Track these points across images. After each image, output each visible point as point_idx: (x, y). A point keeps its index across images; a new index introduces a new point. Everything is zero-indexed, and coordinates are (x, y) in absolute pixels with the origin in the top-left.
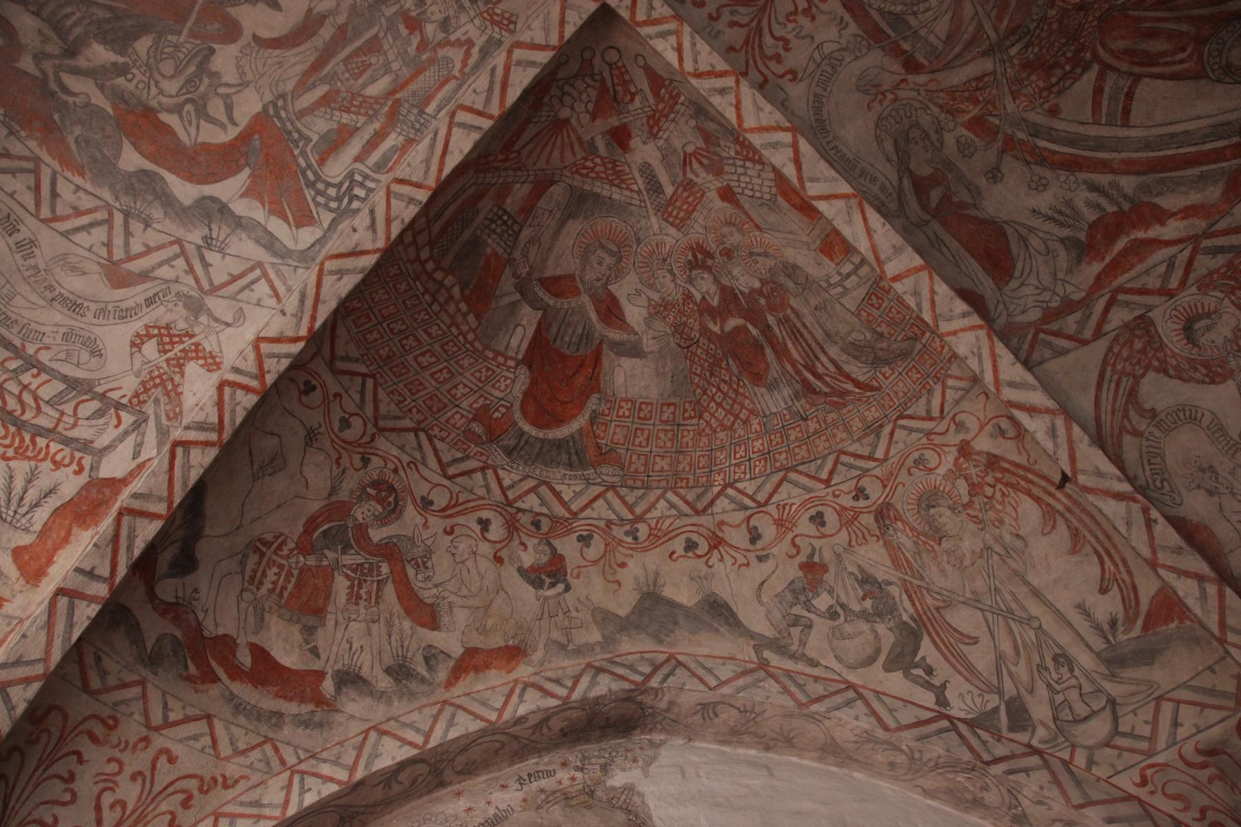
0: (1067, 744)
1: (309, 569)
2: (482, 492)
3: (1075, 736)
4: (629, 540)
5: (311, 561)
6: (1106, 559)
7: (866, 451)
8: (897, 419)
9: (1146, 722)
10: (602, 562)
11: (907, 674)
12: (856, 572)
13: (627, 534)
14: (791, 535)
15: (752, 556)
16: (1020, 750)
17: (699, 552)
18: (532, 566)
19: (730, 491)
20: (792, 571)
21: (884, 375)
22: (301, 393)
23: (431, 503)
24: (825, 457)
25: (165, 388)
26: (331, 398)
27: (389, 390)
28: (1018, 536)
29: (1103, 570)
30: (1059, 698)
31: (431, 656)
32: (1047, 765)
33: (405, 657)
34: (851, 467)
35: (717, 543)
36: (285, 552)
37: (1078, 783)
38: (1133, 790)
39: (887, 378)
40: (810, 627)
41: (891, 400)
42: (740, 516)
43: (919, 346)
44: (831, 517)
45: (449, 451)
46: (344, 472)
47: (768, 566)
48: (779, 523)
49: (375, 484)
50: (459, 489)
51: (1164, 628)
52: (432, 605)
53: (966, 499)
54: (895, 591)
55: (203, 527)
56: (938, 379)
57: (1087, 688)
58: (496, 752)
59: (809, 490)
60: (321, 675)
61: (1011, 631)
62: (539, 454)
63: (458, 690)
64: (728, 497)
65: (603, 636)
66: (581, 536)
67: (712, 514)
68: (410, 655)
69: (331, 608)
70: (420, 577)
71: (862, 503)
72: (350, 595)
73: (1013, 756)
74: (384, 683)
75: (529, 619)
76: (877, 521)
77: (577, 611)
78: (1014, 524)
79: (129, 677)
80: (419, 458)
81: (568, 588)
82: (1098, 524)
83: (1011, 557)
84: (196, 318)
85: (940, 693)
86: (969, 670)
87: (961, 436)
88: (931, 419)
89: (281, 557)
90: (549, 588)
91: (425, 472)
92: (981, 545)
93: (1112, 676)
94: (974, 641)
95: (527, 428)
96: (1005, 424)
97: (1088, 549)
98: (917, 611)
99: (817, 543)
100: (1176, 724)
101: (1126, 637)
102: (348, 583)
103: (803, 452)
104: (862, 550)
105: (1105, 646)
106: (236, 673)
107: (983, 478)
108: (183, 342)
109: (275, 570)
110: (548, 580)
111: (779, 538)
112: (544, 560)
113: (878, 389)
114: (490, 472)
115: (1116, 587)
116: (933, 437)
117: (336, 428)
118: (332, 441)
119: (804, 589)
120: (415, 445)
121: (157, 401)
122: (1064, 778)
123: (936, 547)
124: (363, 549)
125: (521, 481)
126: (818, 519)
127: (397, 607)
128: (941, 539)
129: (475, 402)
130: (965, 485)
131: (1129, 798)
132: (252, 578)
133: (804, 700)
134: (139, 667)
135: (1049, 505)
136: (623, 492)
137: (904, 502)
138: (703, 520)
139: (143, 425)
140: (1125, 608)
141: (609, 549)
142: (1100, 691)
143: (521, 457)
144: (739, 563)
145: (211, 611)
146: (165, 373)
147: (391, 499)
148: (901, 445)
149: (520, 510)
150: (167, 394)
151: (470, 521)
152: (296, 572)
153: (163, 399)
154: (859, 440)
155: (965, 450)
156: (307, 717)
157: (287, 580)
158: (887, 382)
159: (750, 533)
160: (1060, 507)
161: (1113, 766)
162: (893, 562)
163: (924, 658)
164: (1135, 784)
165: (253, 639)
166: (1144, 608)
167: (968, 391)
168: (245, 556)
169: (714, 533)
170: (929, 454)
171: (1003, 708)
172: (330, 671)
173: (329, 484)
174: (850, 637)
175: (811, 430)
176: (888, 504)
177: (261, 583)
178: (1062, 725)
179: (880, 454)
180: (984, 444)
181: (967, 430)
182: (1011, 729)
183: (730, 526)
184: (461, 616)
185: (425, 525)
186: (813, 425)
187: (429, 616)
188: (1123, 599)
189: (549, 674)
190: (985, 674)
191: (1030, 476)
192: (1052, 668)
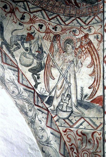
0: (56, 114)
3: (59, 113)
6: (96, 81)
7: (64, 19)
8: (77, 18)
9: (76, 120)
11: (33, 75)
12: (40, 45)
14: (31, 25)
15: (18, 22)
16: (44, 107)
17: (6, 10)
19: (25, 3)
20: (25, 33)
21: (83, 5)
24: (54, 14)
28: (82, 63)
29: (93, 83)
30: (62, 103)
32: (48, 114)
34: (58, 20)
35: (12, 12)
37: (51, 122)
38: (61, 132)
39: (83, 6)
40: (19, 48)
41: (80, 12)
42: (23, 10)
43: (97, 3)
44: (44, 28)
47: (21, 27)
48: (31, 20)
51: (95, 104)
53: (77, 47)
54: (45, 55)
56: (94, 15)
57: (69, 105)
59: (44, 18)
61: (63, 82)
64: (24, 3)
67: (17, 4)
71: (54, 31)
73: (42, 108)
76: (54, 37)
78: (83, 60)
82: (100, 73)
83: (76, 67)
85: (37, 84)
86: (47, 84)
87: (88, 32)
88: (85, 23)
92: (72, 60)
93: (77, 107)
94: (54, 79)
96: (100, 36)
97: (94, 77)
98: (46, 63)
99: (36, 31)
100: (81, 124)
101: (86, 101)
103: (50, 8)
104: (45, 41)
105: (80, 99)
107: (85, 45)
111: (28, 23)
113: (79, 7)
115: (93, 89)
116: (82, 28)
119: (25, 39)
122: (49, 119)
123: (62, 53)
126: (41, 26)
128: (64, 52)
130: (80, 44)
131: (60, 132)
133: (4, 61)
135: (94, 61)
137: (64, 37)
138: (13, 4)
140: (91, 95)
142: (72, 108)
144: (14, 21)
148: (73, 25)
154: (65, 16)
155: (86, 36)
158: (82, 7)
159: (22, 16)
160: (96, 64)
161: (61, 124)
162: (50, 49)
163: (39, 74)
164: (63, 131)
166: (95, 97)
167: (98, 23)
169: (13, 9)
170: (78, 31)
171: (48, 97)
174: (26, 57)
175: (56, 5)
176: (59, 35)
178: (58, 109)
179: (67, 23)
180: (91, 38)
181: (91, 32)
182: (46, 102)
183: (19, 11)
186: (57, 4)
188: (92, 92)
190: (50, 87)
191: (95, 52)
192: (65, 96)
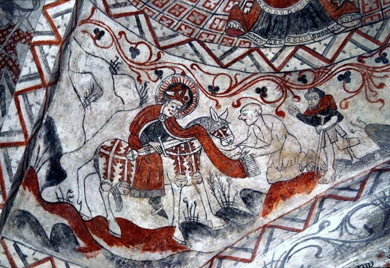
1: (143, 158)
2: (254, 69)
4: (381, 64)
5: (143, 152)
10: (363, 89)
13: (377, 61)
18: (307, 111)
22: (94, 39)
23: (217, 89)
25: (8, 65)
26: (118, 37)
27: (158, 18)
31: (248, 196)
33: (228, 202)
36: (123, 151)
45: (219, 48)
46: (146, 85)
49: (170, 88)
50: (234, 73)
52: (239, 160)
55: (61, 148)
58: (317, 255)
60: (171, 229)
62: (288, 27)
63: (272, 216)
65: (380, 145)
66: (340, 75)
68: (231, 199)
69: (166, 181)
70: (224, 143)
72: (177, 168)
74: (216, 223)
75: (315, 149)
77: (353, 132)
79: (41, 257)
80: (199, 60)
81: (341, 118)
84: (12, 14)
89: (121, 155)
90: (325, 122)
91: (205, 68)
95: (273, 11)
102: (174, 161)
106: (112, 240)
108: (10, 33)
109: (120, 165)
110: (323, 117)
112: (316, 102)
114: (255, 54)
117: (130, 57)
118: (130, 66)
120: (193, 52)
121: (6, 76)
124: (176, 135)
125: (281, 51)
127: (214, 169)
129: (227, 6)
132: (106, 174)
134: (45, 248)
136: (365, 29)
139: (3, 93)
141: (367, 78)
143: (275, 34)
145: (84, 203)
146: (6, 56)
147: (187, 94)
149: (286, 73)
150: (10, 68)
151: (251, 93)
152: (134, 163)
153: (10, 73)
156: (168, 260)
157: (129, 169)
165: (118, 215)
168: (96, 161)
172: (177, 225)
173: (138, 96)
177: (112, 176)
184: (262, 162)
185: (218, 105)
187: (239, 168)
189: (340, 186)
